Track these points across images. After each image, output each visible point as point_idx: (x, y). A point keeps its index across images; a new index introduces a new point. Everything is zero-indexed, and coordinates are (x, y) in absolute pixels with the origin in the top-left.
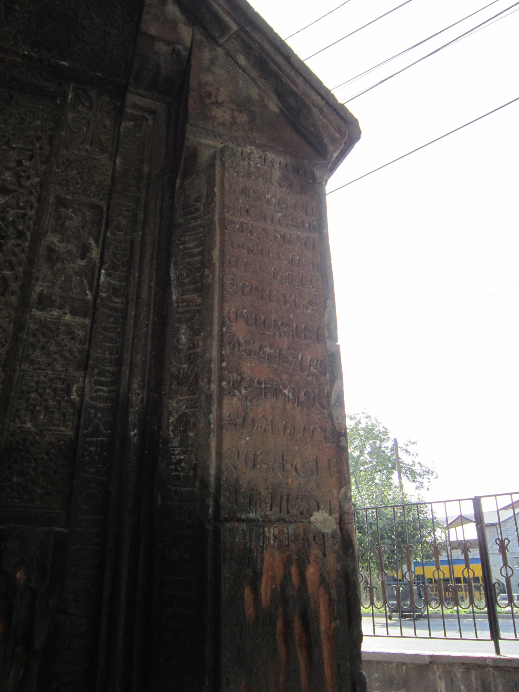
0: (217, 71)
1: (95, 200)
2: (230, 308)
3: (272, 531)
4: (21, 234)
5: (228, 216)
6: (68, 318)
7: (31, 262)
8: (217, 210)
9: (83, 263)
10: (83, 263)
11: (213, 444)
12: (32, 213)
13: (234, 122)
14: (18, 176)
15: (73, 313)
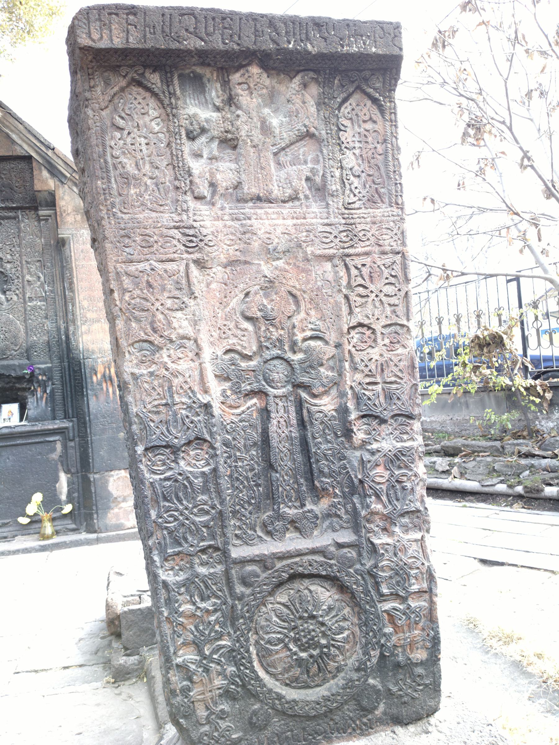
0: (66, 197)
1: (38, 259)
2: (81, 297)
3: (99, 360)
4: (18, 277)
5: (77, 263)
6: (39, 303)
7: (23, 287)
8: (73, 262)
9: (39, 283)
10: (39, 283)
11: (80, 339)
12: (19, 269)
13: (76, 221)
14: (11, 255)
15: (40, 301)
